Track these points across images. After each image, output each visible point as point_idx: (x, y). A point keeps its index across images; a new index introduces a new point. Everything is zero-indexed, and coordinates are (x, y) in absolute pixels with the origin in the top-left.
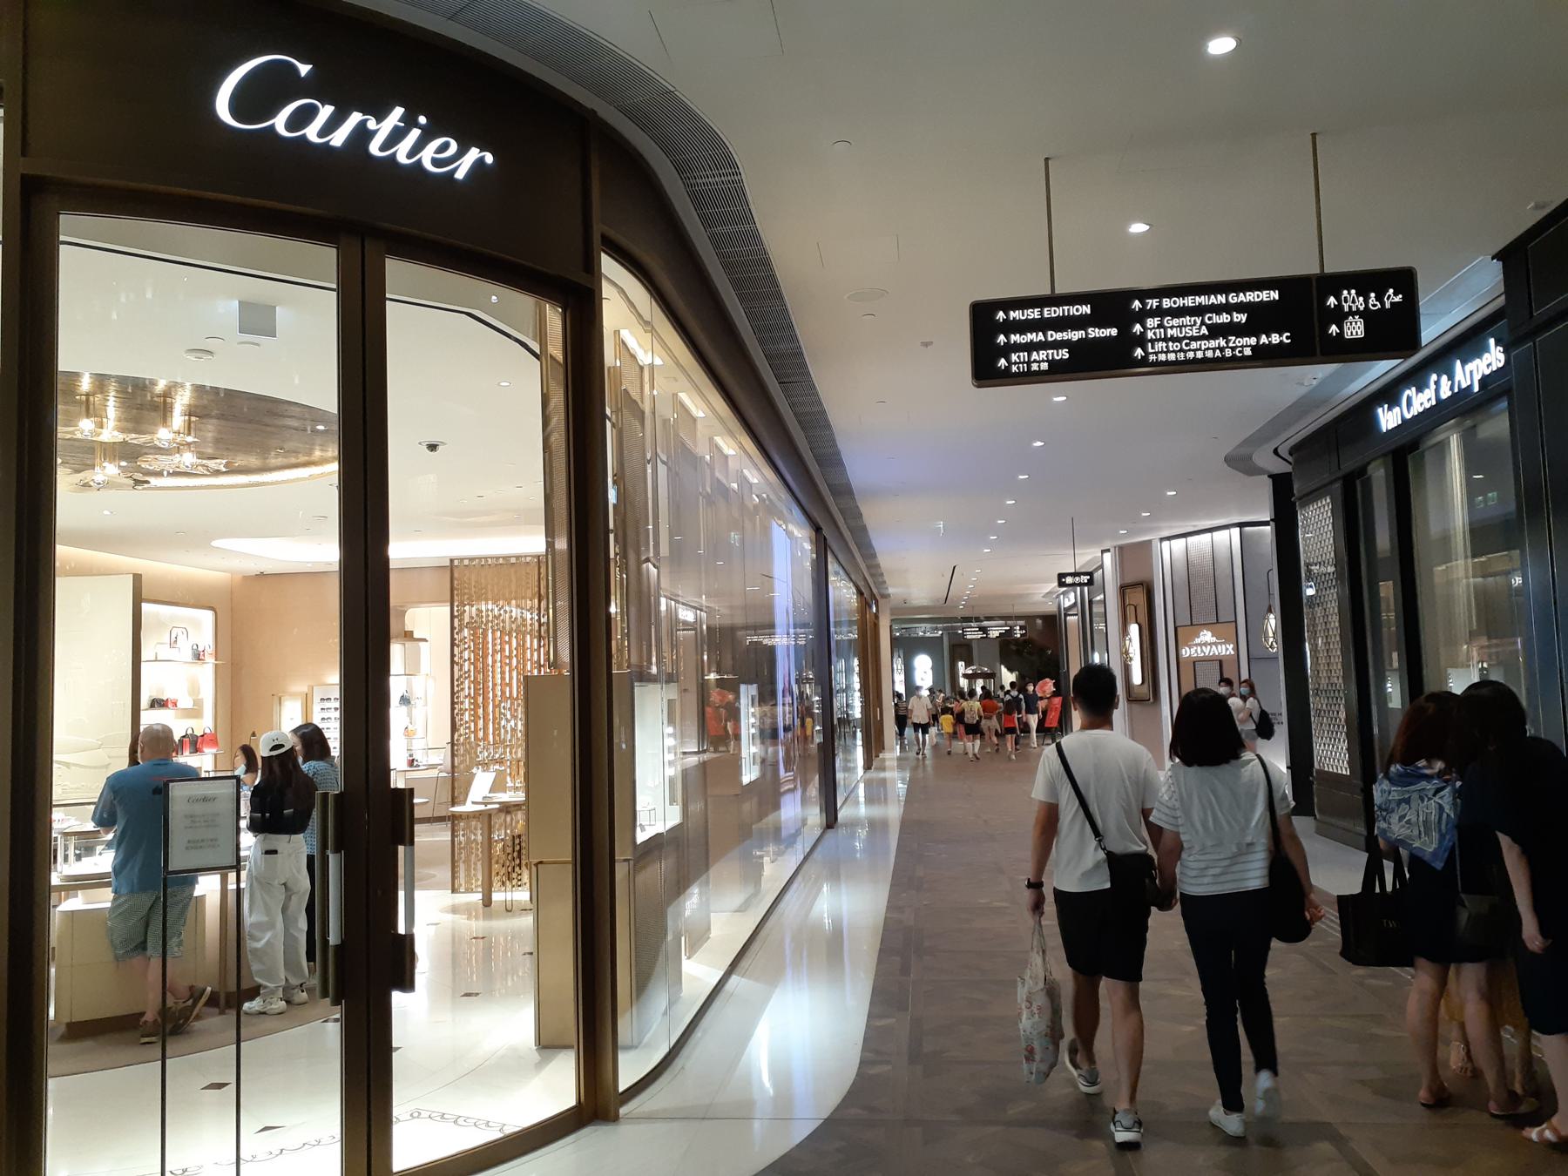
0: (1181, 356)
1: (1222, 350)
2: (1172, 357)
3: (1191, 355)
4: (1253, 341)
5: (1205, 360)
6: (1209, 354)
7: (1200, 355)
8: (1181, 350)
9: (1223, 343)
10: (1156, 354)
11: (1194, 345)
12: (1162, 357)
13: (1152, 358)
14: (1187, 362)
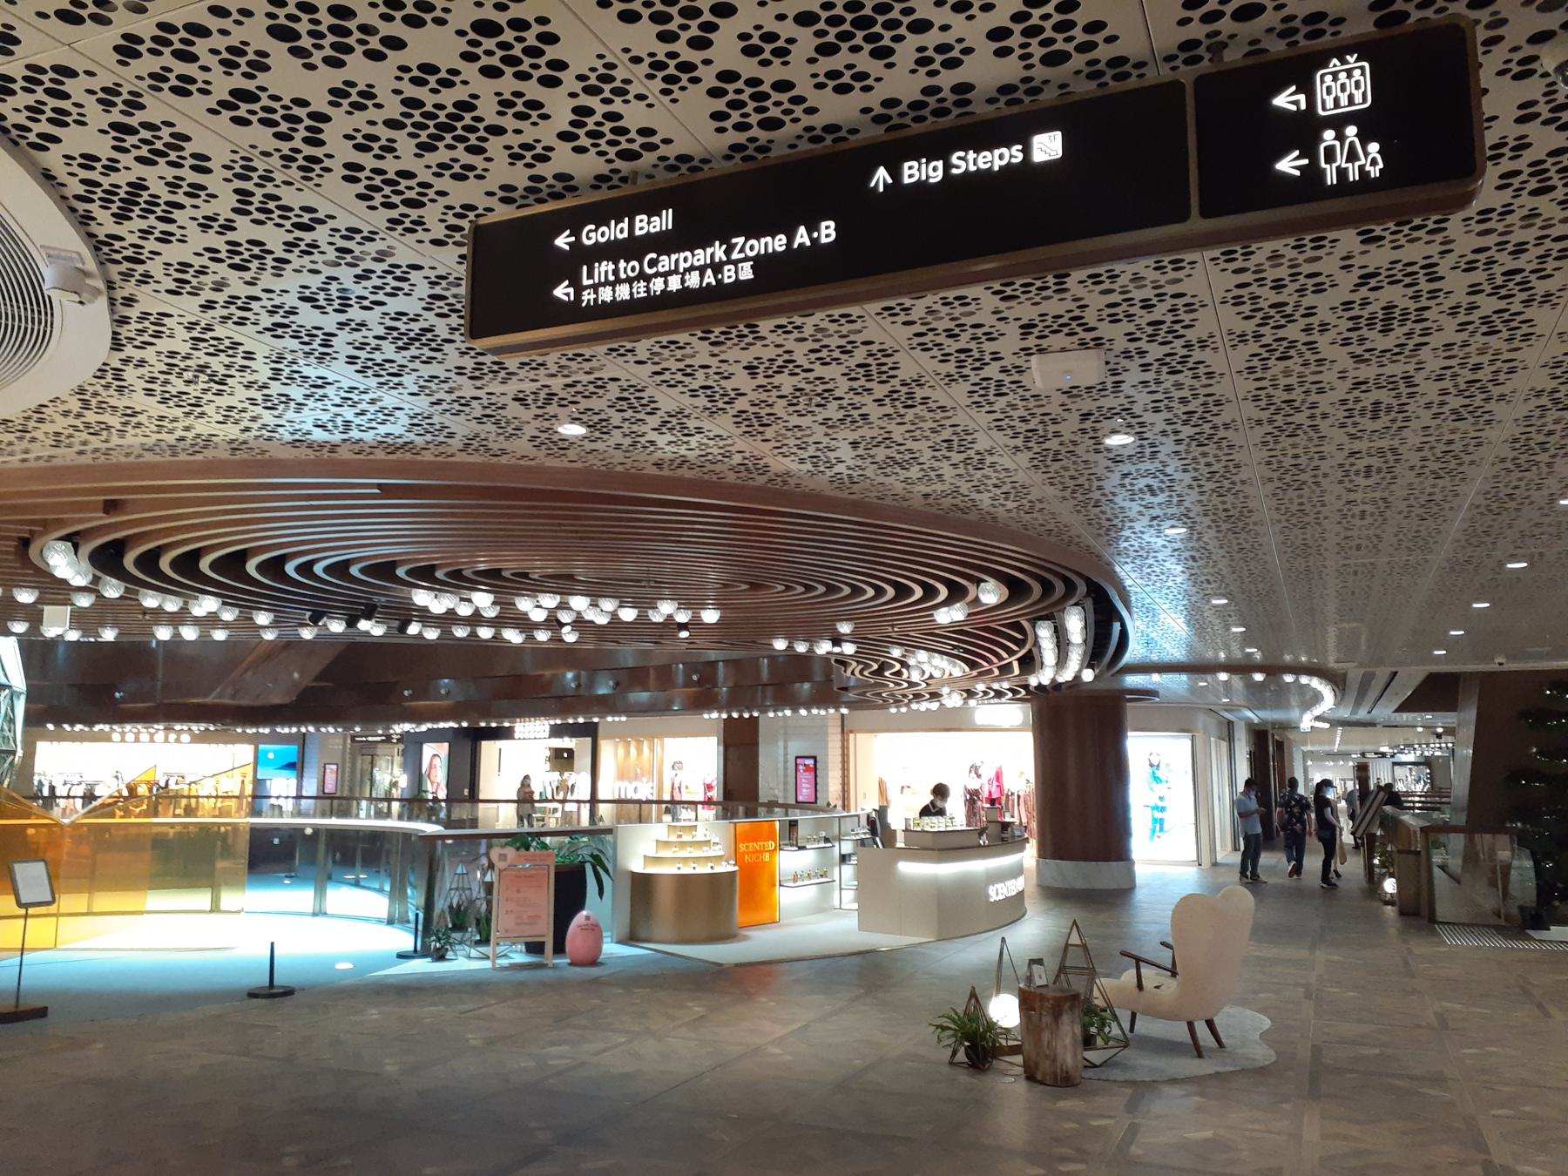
0: (640, 290)
1: (717, 268)
2: (623, 292)
3: (658, 285)
7: (674, 284)
8: (642, 276)
9: (720, 254)
10: (595, 287)
11: (666, 263)
12: (606, 294)
13: (588, 296)
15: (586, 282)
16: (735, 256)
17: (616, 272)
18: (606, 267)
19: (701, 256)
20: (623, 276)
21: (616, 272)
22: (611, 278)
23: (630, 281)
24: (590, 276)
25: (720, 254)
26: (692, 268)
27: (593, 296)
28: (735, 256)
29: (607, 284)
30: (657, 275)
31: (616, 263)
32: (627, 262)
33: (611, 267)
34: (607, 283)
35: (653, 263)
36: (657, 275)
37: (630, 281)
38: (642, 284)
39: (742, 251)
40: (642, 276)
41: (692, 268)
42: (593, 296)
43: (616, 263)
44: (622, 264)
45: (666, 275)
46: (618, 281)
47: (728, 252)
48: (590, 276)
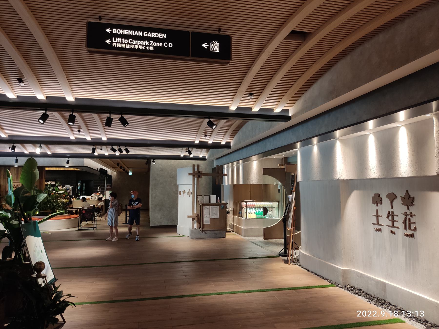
0: (128, 46)
1: (146, 46)
2: (123, 46)
3: (132, 46)
4: (161, 45)
5: (139, 50)
6: (141, 47)
7: (136, 47)
8: (128, 43)
9: (147, 43)
10: (116, 43)
11: (134, 42)
12: (119, 45)
13: (114, 45)
14: (130, 49)
15: (114, 41)
16: (151, 45)
17: (122, 41)
18: (118, 40)
19: (143, 43)
20: (123, 42)
21: (122, 41)
22: (120, 42)
23: (126, 44)
24: (115, 40)
25: (147, 43)
26: (141, 45)
27: (115, 45)
28: (151, 45)
29: (118, 43)
30: (132, 44)
31: (122, 39)
32: (125, 39)
33: (120, 40)
34: (119, 43)
35: (131, 41)
36: (132, 44)
37: (126, 44)
38: (128, 45)
39: (152, 44)
40: (128, 43)
41: (141, 45)
42: (115, 45)
43: (122, 39)
44: (123, 40)
45: (134, 44)
46: (122, 43)
47: (150, 43)
48: (115, 40)
